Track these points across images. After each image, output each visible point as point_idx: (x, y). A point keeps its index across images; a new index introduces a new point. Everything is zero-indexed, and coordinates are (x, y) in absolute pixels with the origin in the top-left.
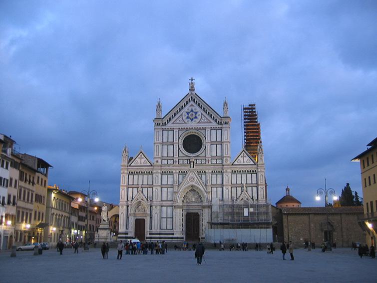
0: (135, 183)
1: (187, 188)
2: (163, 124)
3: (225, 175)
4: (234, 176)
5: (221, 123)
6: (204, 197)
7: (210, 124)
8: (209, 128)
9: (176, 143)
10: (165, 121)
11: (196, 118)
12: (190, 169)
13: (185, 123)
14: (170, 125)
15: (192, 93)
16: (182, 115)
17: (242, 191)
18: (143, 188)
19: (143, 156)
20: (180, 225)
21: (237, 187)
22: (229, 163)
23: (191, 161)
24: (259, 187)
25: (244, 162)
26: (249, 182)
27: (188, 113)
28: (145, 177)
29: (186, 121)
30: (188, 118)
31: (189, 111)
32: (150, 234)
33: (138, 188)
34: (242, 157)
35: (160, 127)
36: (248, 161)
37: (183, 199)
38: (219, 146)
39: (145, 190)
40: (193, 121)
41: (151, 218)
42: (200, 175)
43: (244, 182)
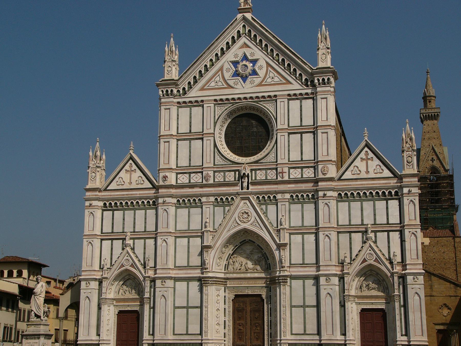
2: (178, 91)
4: (344, 206)
6: (274, 258)
7: (289, 87)
12: (241, 191)
14: (194, 93)
15: (244, 19)
16: (221, 69)
17: (364, 242)
19: (134, 167)
21: (350, 232)
24: (407, 232)
25: (367, 172)
26: (382, 219)
27: (235, 63)
28: (140, 213)
29: (231, 83)
34: (362, 159)
36: (379, 170)
38: (308, 138)
42: (264, 207)
43: (368, 221)
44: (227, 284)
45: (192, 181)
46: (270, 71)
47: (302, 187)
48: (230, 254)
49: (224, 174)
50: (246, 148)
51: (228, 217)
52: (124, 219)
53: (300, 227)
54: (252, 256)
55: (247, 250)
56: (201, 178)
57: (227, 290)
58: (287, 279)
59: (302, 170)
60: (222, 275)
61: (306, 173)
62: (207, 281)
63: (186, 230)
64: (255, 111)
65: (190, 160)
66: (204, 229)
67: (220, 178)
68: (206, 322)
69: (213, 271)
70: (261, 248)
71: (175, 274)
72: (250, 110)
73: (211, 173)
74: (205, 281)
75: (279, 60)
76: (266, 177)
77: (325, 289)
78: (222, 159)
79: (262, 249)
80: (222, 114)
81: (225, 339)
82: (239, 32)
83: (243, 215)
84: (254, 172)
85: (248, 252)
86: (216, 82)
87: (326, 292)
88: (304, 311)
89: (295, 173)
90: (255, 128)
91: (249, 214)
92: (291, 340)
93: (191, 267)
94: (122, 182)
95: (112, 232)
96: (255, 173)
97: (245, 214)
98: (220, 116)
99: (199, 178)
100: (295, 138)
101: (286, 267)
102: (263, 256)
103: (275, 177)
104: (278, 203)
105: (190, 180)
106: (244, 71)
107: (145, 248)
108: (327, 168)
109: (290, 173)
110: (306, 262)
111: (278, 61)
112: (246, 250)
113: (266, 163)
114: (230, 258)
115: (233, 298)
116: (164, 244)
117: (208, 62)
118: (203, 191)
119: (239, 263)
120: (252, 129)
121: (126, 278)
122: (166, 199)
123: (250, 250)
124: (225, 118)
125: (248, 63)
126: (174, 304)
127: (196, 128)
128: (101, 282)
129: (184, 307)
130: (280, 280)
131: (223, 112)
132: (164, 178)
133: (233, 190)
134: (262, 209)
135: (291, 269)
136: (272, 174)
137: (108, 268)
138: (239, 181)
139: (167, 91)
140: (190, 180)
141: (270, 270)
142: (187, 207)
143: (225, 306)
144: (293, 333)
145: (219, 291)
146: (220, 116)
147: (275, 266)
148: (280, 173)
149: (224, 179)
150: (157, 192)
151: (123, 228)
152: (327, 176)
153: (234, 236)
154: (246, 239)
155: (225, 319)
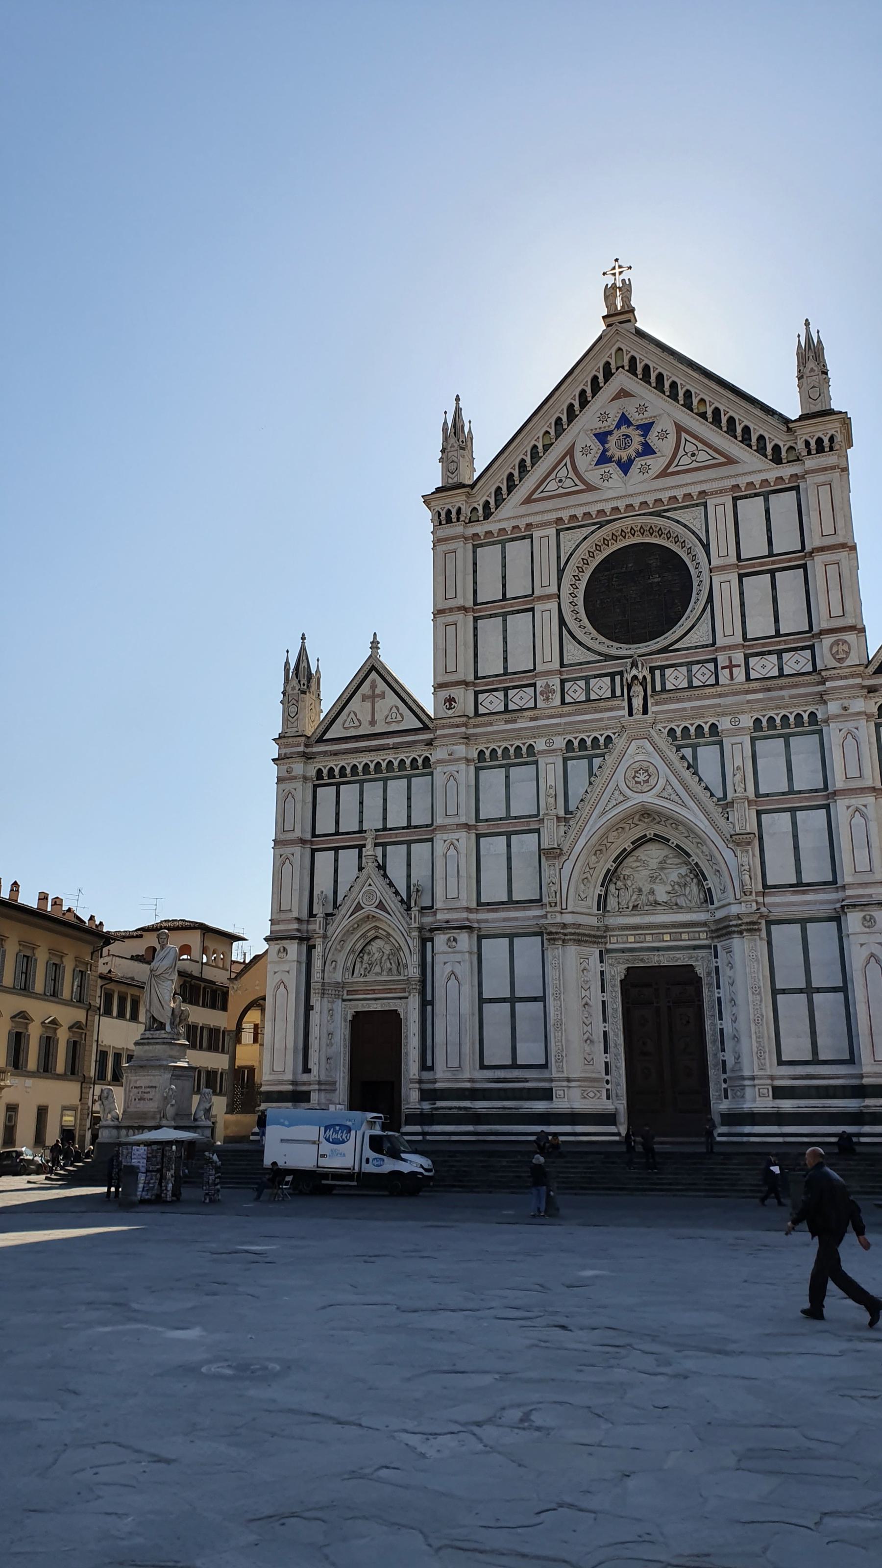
0: (349, 824)
1: (618, 826)
3: (833, 734)
5: (791, 448)
8: (721, 492)
9: (548, 597)
10: (484, 494)
11: (647, 450)
13: (590, 488)
16: (570, 452)
18: (384, 845)
19: (381, 686)
20: (589, 1040)
22: (853, 660)
23: (625, 675)
27: (602, 437)
28: (397, 787)
29: (593, 476)
30: (604, 459)
31: (611, 423)
32: (428, 1095)
33: (361, 847)
35: (457, 529)
37: (598, 890)
38: (790, 582)
39: (396, 857)
40: (634, 469)
41: (426, 1003)
42: (688, 752)
44: (606, 943)
45: (511, 706)
46: (686, 440)
47: (783, 698)
48: (609, 870)
49: (587, 684)
50: (636, 623)
51: (598, 782)
52: (361, 803)
53: (783, 794)
54: (665, 874)
55: (651, 860)
56: (533, 699)
57: (606, 957)
58: (760, 923)
59: (780, 658)
60: (593, 921)
61: (792, 663)
62: (557, 933)
63: (501, 819)
64: (656, 537)
65: (505, 659)
66: (541, 813)
67: (578, 694)
68: (560, 1034)
69: (569, 909)
71: (478, 921)
72: (643, 534)
73: (555, 682)
74: (550, 933)
75: (706, 413)
76: (690, 682)
77: (862, 945)
78: (579, 649)
79: (689, 856)
80: (574, 550)
81: (608, 1077)
82: (607, 364)
83: (637, 775)
84: (657, 673)
85: (654, 864)
86: (560, 481)
87: (865, 953)
88: (810, 1002)
89: (763, 667)
90: (657, 576)
91: (652, 770)
92: (782, 1077)
93: (517, 902)
94: (354, 718)
95: (337, 833)
96: (663, 676)
97: (642, 772)
98: (571, 555)
99: (526, 697)
100: (757, 587)
101: (754, 894)
102: (691, 873)
103: (712, 681)
104: (724, 739)
105: (506, 706)
106: (625, 449)
107: (409, 865)
108: (846, 642)
109: (750, 667)
110: (805, 880)
111: (703, 415)
113: (688, 649)
114: (611, 880)
115: (623, 977)
116: (452, 851)
117: (538, 438)
118: (538, 727)
119: (634, 892)
120: (649, 578)
121: (369, 934)
122: (455, 747)
123: (658, 860)
124: (583, 559)
125: (630, 431)
126: (480, 993)
127: (518, 587)
128: (311, 948)
129: (503, 1000)
130: (740, 925)
131: (578, 546)
132: (447, 704)
133: (609, 718)
134: (683, 758)
135: (768, 900)
136: (703, 674)
137: (327, 915)
138: (622, 695)
139: (449, 512)
140: (506, 706)
141: (712, 903)
142: (500, 766)
143: (603, 997)
144: (784, 1058)
145: (587, 960)
146: (571, 555)
148: (723, 668)
149: (588, 694)
150: (431, 736)
151: (361, 822)
152: (845, 664)
153: (617, 827)
154: (647, 833)
155: (605, 1027)
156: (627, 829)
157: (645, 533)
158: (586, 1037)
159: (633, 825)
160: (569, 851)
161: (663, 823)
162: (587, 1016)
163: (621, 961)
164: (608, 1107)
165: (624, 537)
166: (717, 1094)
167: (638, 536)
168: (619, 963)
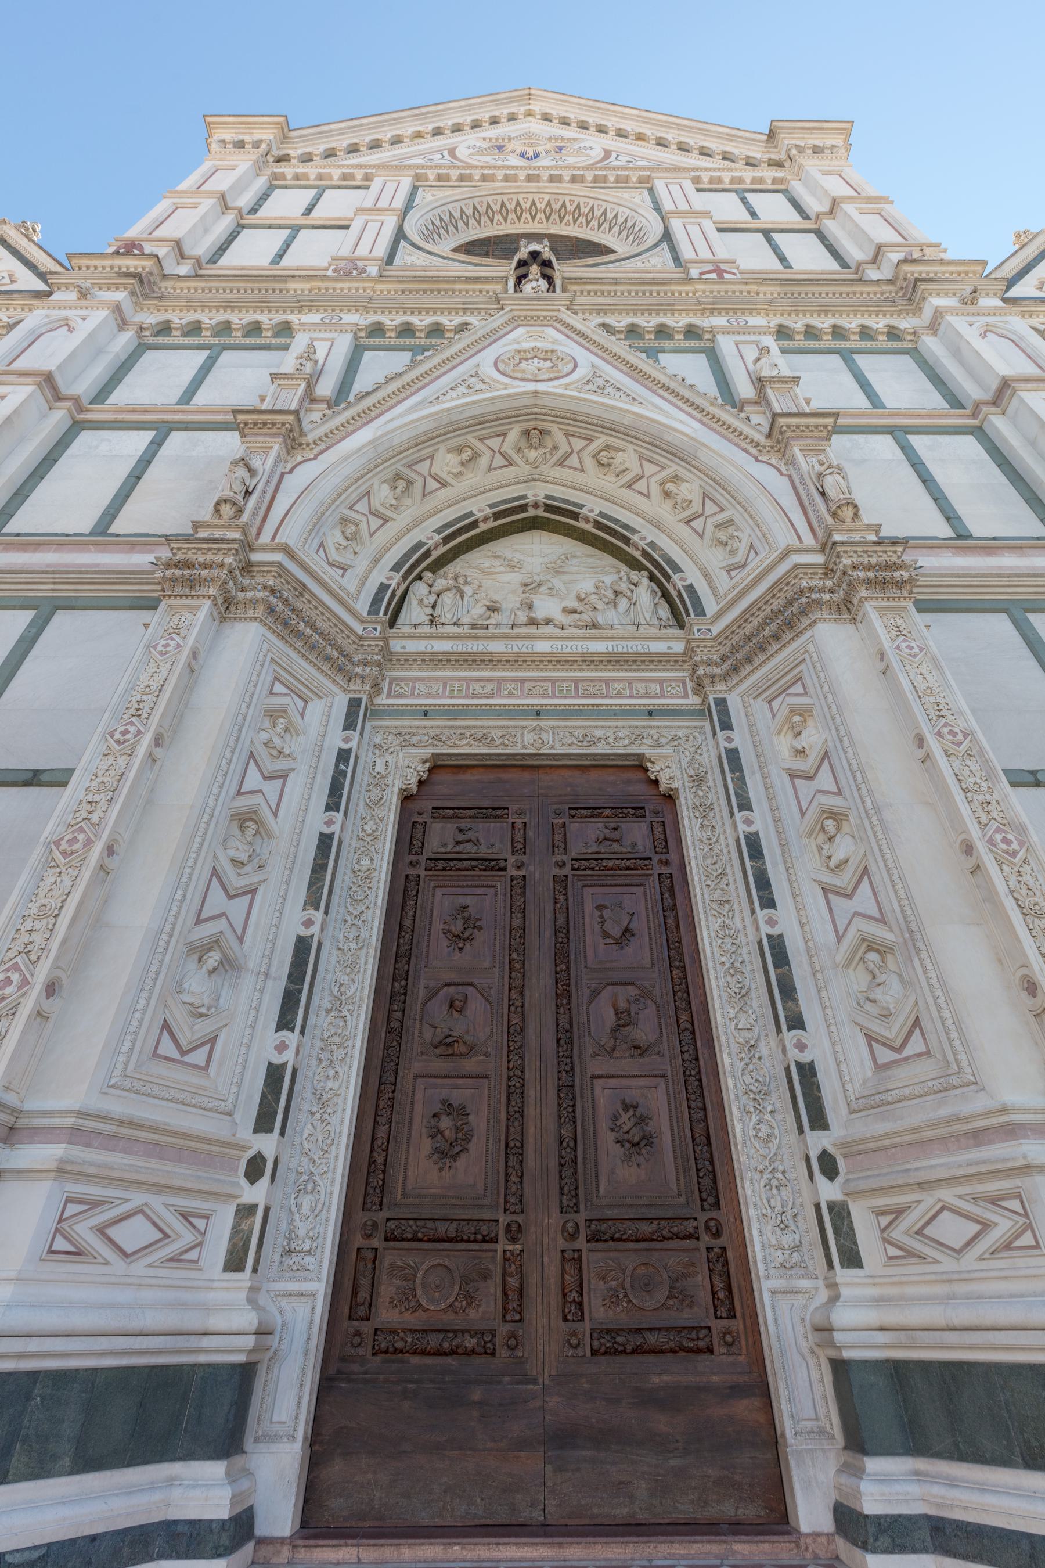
48: (419, 545)
64: (568, 224)
70: (626, 527)
72: (548, 218)
112: (522, 558)
123: (546, 560)
141: (703, 613)
145: (300, 703)
147: (744, 566)
156: (484, 461)
157: (553, 216)
158: (208, 930)
159: (499, 461)
160: (323, 446)
161: (574, 461)
162: (244, 857)
163: (414, 740)
164: (217, 1322)
165: (519, 218)
166: (788, 1240)
167: (540, 222)
168: (408, 744)
